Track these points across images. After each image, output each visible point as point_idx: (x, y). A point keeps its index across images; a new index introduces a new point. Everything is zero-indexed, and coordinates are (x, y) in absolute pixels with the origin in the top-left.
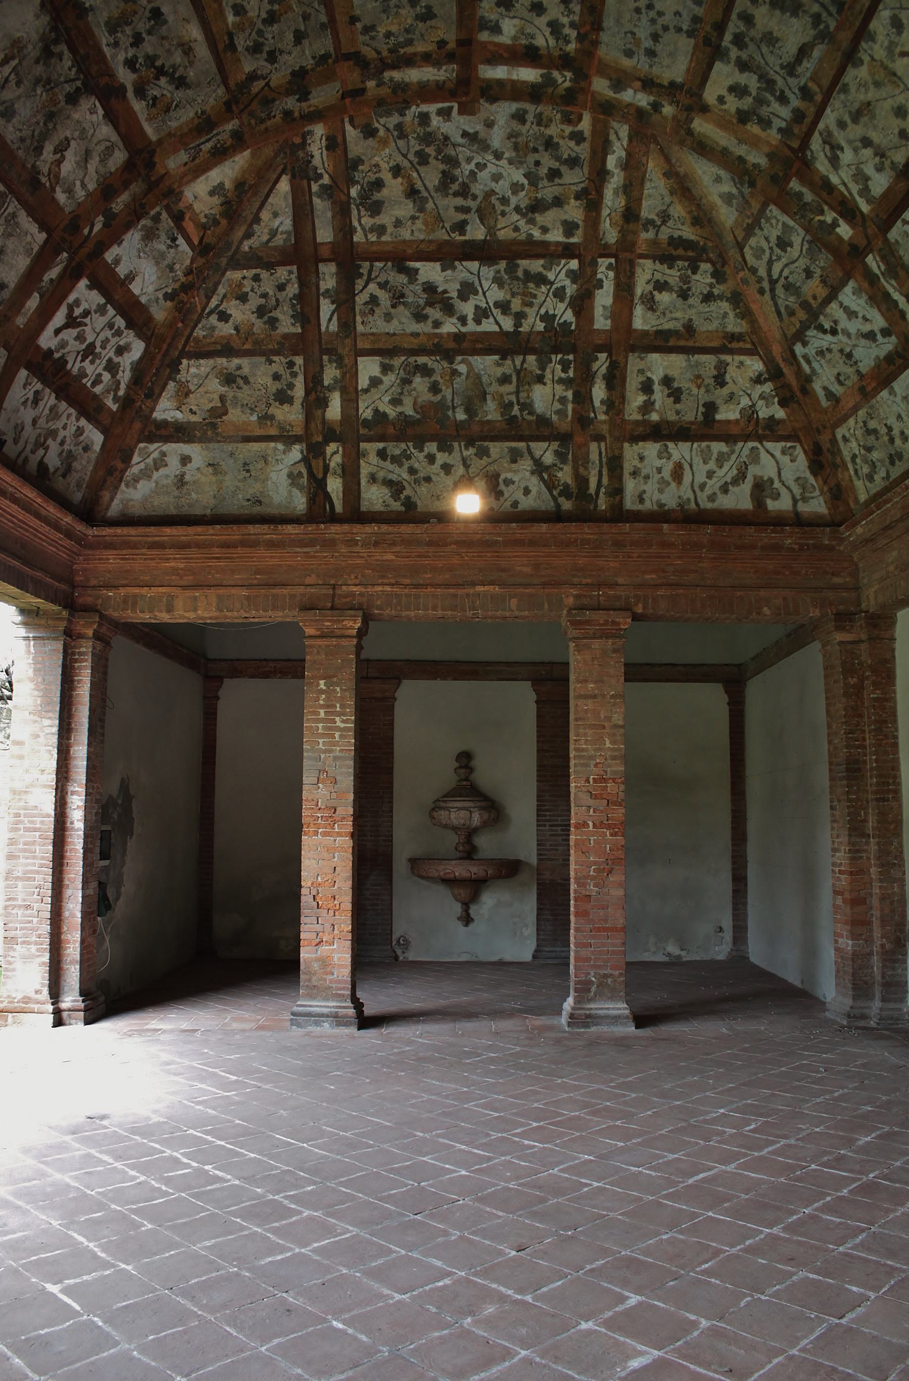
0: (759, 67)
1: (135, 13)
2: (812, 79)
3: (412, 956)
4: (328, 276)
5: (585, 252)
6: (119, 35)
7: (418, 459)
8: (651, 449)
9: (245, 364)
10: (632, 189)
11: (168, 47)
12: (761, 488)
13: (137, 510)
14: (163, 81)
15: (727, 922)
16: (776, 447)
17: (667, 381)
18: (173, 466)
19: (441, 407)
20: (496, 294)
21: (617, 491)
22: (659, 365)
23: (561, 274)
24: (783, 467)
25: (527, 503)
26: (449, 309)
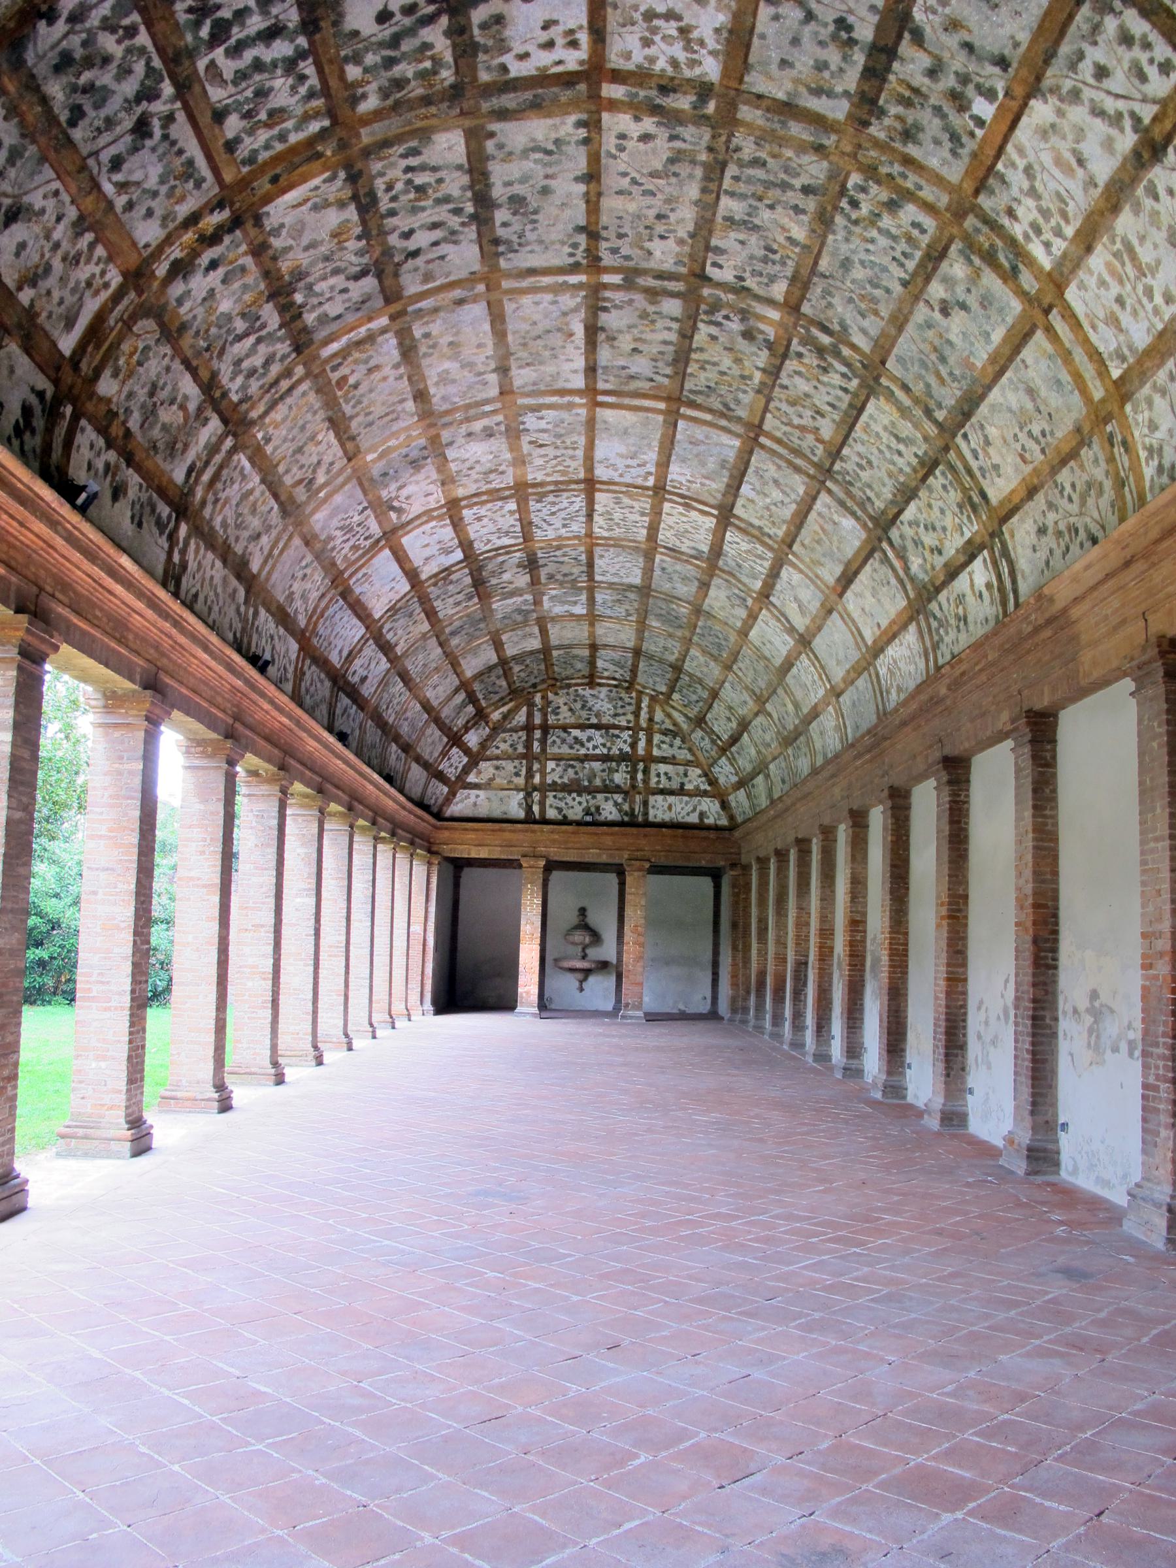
3: (553, 1006)
4: (538, 734)
5: (635, 729)
7: (569, 799)
8: (660, 798)
12: (702, 815)
13: (457, 814)
15: (709, 995)
16: (708, 800)
18: (473, 799)
21: (646, 814)
22: (663, 768)
23: (626, 735)
25: (610, 818)
26: (582, 745)
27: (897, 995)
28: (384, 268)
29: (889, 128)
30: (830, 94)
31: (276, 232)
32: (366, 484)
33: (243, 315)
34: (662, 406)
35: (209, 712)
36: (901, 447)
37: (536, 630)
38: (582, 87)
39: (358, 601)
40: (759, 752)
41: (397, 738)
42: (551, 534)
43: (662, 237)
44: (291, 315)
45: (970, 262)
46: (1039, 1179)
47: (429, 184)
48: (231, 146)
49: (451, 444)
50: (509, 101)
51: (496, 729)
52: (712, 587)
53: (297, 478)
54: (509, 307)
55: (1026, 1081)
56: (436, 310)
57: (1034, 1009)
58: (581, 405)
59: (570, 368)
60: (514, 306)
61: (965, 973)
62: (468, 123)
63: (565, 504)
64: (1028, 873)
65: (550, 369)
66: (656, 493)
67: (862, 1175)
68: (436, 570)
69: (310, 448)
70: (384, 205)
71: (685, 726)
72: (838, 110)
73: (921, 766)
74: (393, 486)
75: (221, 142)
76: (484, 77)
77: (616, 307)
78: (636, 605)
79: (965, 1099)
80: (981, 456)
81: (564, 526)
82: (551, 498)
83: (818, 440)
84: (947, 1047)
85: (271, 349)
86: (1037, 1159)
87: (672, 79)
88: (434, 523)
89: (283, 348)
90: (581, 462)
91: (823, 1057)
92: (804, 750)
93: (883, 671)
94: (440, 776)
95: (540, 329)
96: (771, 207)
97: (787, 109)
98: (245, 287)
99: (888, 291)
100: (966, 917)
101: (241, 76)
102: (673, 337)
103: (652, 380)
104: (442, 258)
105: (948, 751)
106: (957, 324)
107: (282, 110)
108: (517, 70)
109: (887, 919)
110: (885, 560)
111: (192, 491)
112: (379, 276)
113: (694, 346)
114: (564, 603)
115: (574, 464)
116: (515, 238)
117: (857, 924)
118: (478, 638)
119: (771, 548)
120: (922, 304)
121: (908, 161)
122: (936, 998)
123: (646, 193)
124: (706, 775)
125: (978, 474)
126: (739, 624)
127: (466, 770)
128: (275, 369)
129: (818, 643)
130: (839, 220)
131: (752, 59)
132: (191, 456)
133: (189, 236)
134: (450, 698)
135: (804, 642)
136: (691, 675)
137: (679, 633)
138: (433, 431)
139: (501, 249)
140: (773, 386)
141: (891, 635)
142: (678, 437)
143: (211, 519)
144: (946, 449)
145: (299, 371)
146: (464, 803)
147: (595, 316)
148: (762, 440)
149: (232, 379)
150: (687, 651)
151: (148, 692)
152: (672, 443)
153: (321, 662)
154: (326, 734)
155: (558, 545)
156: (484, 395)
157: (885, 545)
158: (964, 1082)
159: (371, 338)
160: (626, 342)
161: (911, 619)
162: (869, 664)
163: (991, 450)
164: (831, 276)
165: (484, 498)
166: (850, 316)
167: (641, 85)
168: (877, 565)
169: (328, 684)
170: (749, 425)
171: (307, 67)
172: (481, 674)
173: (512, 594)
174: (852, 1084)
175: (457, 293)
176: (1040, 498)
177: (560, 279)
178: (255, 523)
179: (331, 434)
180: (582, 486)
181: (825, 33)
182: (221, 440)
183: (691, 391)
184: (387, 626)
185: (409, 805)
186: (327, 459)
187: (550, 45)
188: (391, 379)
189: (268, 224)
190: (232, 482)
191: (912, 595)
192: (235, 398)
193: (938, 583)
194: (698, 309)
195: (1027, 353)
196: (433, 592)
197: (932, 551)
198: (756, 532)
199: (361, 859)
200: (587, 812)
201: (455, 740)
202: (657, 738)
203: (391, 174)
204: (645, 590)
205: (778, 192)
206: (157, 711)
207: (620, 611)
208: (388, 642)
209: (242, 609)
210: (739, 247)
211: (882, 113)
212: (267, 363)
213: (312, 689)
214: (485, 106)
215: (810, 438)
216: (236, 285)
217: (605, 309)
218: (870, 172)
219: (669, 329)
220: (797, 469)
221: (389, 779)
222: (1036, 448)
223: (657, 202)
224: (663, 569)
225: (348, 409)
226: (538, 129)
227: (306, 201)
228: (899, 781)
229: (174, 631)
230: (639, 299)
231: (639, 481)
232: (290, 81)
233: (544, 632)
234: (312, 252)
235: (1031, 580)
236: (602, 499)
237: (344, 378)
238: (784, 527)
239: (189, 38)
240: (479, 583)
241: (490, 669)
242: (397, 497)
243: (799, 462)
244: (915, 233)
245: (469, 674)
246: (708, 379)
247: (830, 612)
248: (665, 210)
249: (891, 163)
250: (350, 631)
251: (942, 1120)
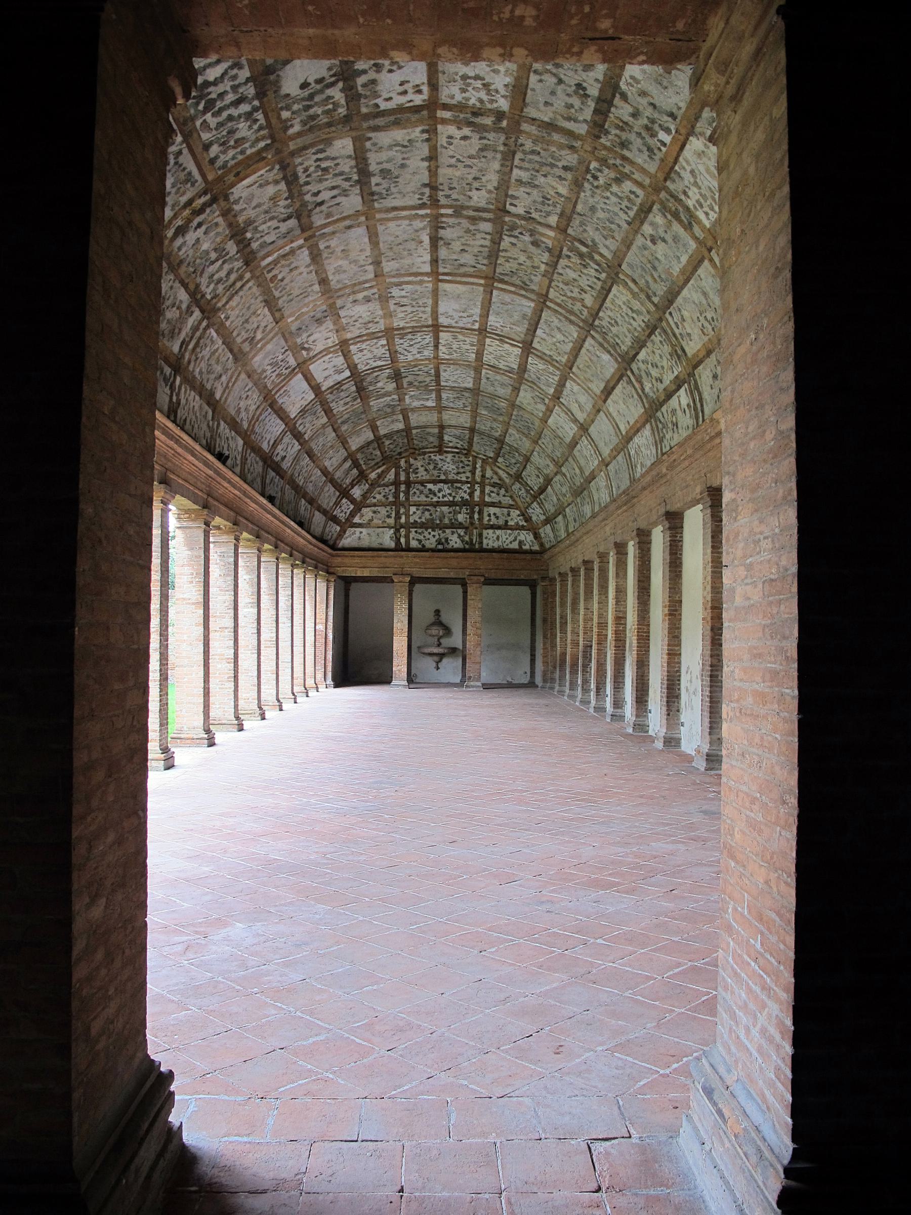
3: (417, 681)
4: (403, 488)
7: (426, 534)
8: (490, 531)
9: (379, 509)
10: (483, 470)
12: (521, 543)
13: (347, 546)
16: (525, 532)
17: (495, 514)
18: (358, 534)
19: (433, 520)
20: (448, 491)
21: (481, 543)
22: (492, 510)
23: (465, 487)
24: (527, 538)
25: (456, 546)
26: (435, 495)
27: (642, 665)
28: (301, 214)
29: (612, 141)
30: (576, 120)
31: (237, 202)
32: (287, 336)
33: (215, 250)
34: (482, 282)
35: (194, 493)
36: (634, 315)
37: (401, 417)
38: (425, 113)
40: (558, 499)
41: (305, 495)
42: (410, 358)
43: (477, 189)
44: (244, 245)
45: (666, 217)
46: (713, 772)
47: (331, 167)
48: (212, 161)
49: (343, 307)
50: (380, 121)
51: (374, 485)
53: (244, 338)
54: (380, 228)
55: (707, 714)
56: (334, 233)
57: (711, 671)
58: (428, 282)
59: (422, 260)
60: (383, 227)
61: (680, 650)
62: (354, 134)
63: (419, 339)
64: (709, 588)
65: (407, 261)
66: (480, 333)
67: (606, 771)
68: (332, 384)
69: (254, 319)
70: (302, 179)
71: (507, 481)
72: (581, 129)
73: (655, 517)
74: (305, 335)
75: (207, 160)
76: (364, 110)
77: (449, 226)
78: (470, 400)
79: (679, 729)
80: (680, 327)
81: (419, 353)
82: (410, 336)
83: (583, 306)
84: (668, 697)
85: (231, 266)
86: (712, 761)
87: (480, 109)
88: (331, 355)
89: (238, 264)
90: (429, 314)
91: (600, 709)
92: (588, 500)
93: (632, 452)
94: (335, 519)
95: (400, 240)
96: (545, 176)
97: (551, 126)
98: (218, 234)
99: (619, 226)
100: (680, 615)
101: (220, 125)
102: (487, 243)
103: (475, 267)
104: (338, 204)
105: (668, 508)
106: (660, 249)
107: (243, 138)
108: (383, 106)
109: (636, 616)
110: (630, 382)
111: (183, 356)
112: (299, 218)
113: (501, 248)
114: (420, 399)
115: (424, 316)
116: (384, 192)
117: (620, 619)
118: (361, 424)
119: (558, 369)
120: (639, 236)
121: (624, 158)
122: (662, 666)
123: (465, 166)
124: (523, 515)
125: (679, 337)
126: (541, 415)
127: (353, 514)
128: (233, 277)
129: (592, 430)
130: (586, 185)
131: (527, 101)
132: (183, 335)
133: (187, 212)
134: (341, 465)
135: (584, 428)
136: (510, 446)
137: (501, 419)
138: (331, 301)
139: (375, 197)
140: (553, 273)
141: (636, 430)
142: (493, 300)
143: (193, 371)
144: (661, 320)
145: (248, 275)
146: (351, 538)
147: (437, 231)
148: (548, 303)
149: (208, 287)
150: (507, 430)
151: (162, 485)
152: (490, 303)
153: (257, 450)
154: (261, 499)
155: (415, 364)
156: (364, 278)
157: (629, 373)
158: (678, 719)
159: (292, 252)
160: (457, 246)
161: (647, 421)
162: (624, 447)
163: (685, 324)
164: (584, 215)
165: (365, 338)
166: (598, 238)
167: (461, 112)
168: (625, 384)
169: (261, 464)
171: (259, 116)
172: (362, 447)
173: (384, 395)
174: (616, 725)
175: (347, 223)
176: (713, 356)
177: (413, 212)
178: (218, 369)
179: (266, 309)
180: (431, 329)
181: (570, 90)
182: (200, 323)
183: (500, 274)
184: (299, 422)
185: (314, 541)
186: (263, 324)
187: (405, 92)
188: (305, 274)
189: (232, 199)
190: (206, 346)
191: (647, 406)
192: (209, 297)
193: (661, 400)
194: (502, 228)
195: (701, 271)
196: (330, 397)
197: (657, 380)
198: (549, 359)
199: (284, 581)
200: (439, 542)
201: (345, 493)
202: (488, 489)
203: (306, 164)
204: (476, 391)
205: (548, 168)
206: (168, 497)
207: (460, 404)
208: (299, 432)
209: (211, 423)
210: (526, 196)
211: (607, 133)
212: (229, 274)
213: (252, 470)
214: (365, 125)
215: (579, 304)
216: (212, 234)
217: (443, 228)
218: (603, 162)
219: (485, 239)
220: (571, 322)
221: (301, 524)
222: (709, 326)
223: (474, 172)
224: (488, 378)
225: (277, 294)
226: (399, 135)
227: (255, 183)
228: (643, 525)
229: (175, 446)
230: (465, 223)
231: (469, 326)
232: (249, 123)
233: (406, 418)
234: (258, 209)
235: (710, 406)
236: (444, 337)
237: (275, 276)
238: (566, 357)
239: (192, 111)
240: (361, 390)
241: (369, 444)
242: (307, 342)
243: (572, 318)
244: (632, 196)
245: (354, 448)
246: (511, 267)
247: (599, 411)
248: (478, 175)
249: (615, 158)
250: (274, 427)
251: (664, 742)
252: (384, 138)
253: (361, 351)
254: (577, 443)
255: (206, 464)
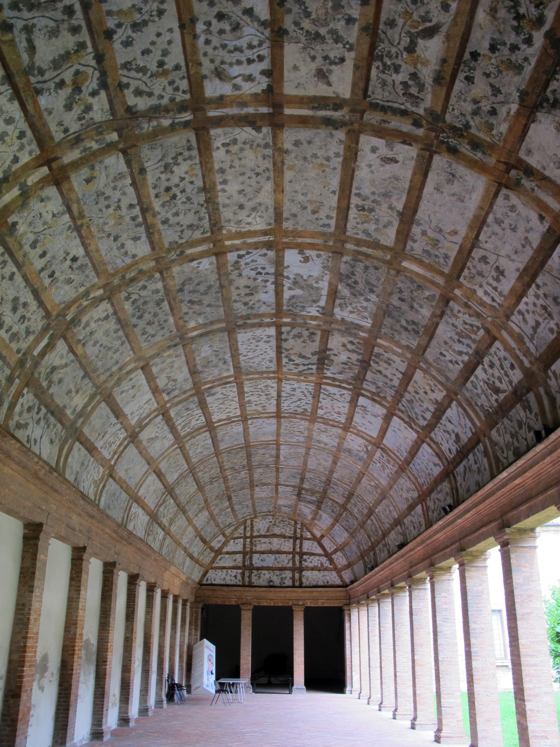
0: (46, 9)
1: (502, 62)
2: (13, 40)
6: (520, 61)
11: (502, 26)
14: (522, 11)
39: (410, 453)
42: (303, 385)
52: (188, 376)
59: (284, 451)
66: (246, 417)
68: (377, 406)
74: (361, 454)
81: (294, 390)
82: (300, 410)
88: (359, 428)
170: (221, 453)
196: (390, 394)
198: (194, 434)
224: (225, 362)
231: (255, 421)
236: (273, 409)
252: (293, 484)
253: (339, 413)
254: (117, 417)
255: (397, 559)
